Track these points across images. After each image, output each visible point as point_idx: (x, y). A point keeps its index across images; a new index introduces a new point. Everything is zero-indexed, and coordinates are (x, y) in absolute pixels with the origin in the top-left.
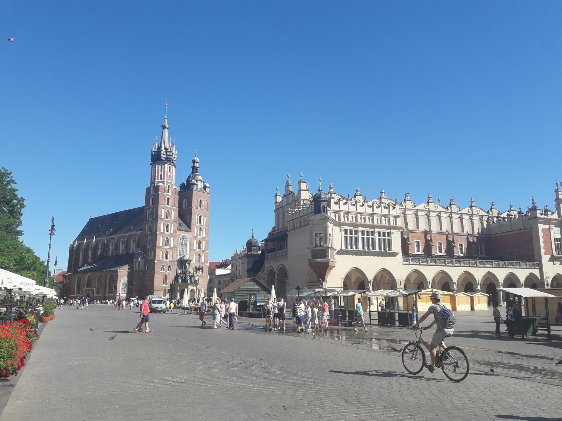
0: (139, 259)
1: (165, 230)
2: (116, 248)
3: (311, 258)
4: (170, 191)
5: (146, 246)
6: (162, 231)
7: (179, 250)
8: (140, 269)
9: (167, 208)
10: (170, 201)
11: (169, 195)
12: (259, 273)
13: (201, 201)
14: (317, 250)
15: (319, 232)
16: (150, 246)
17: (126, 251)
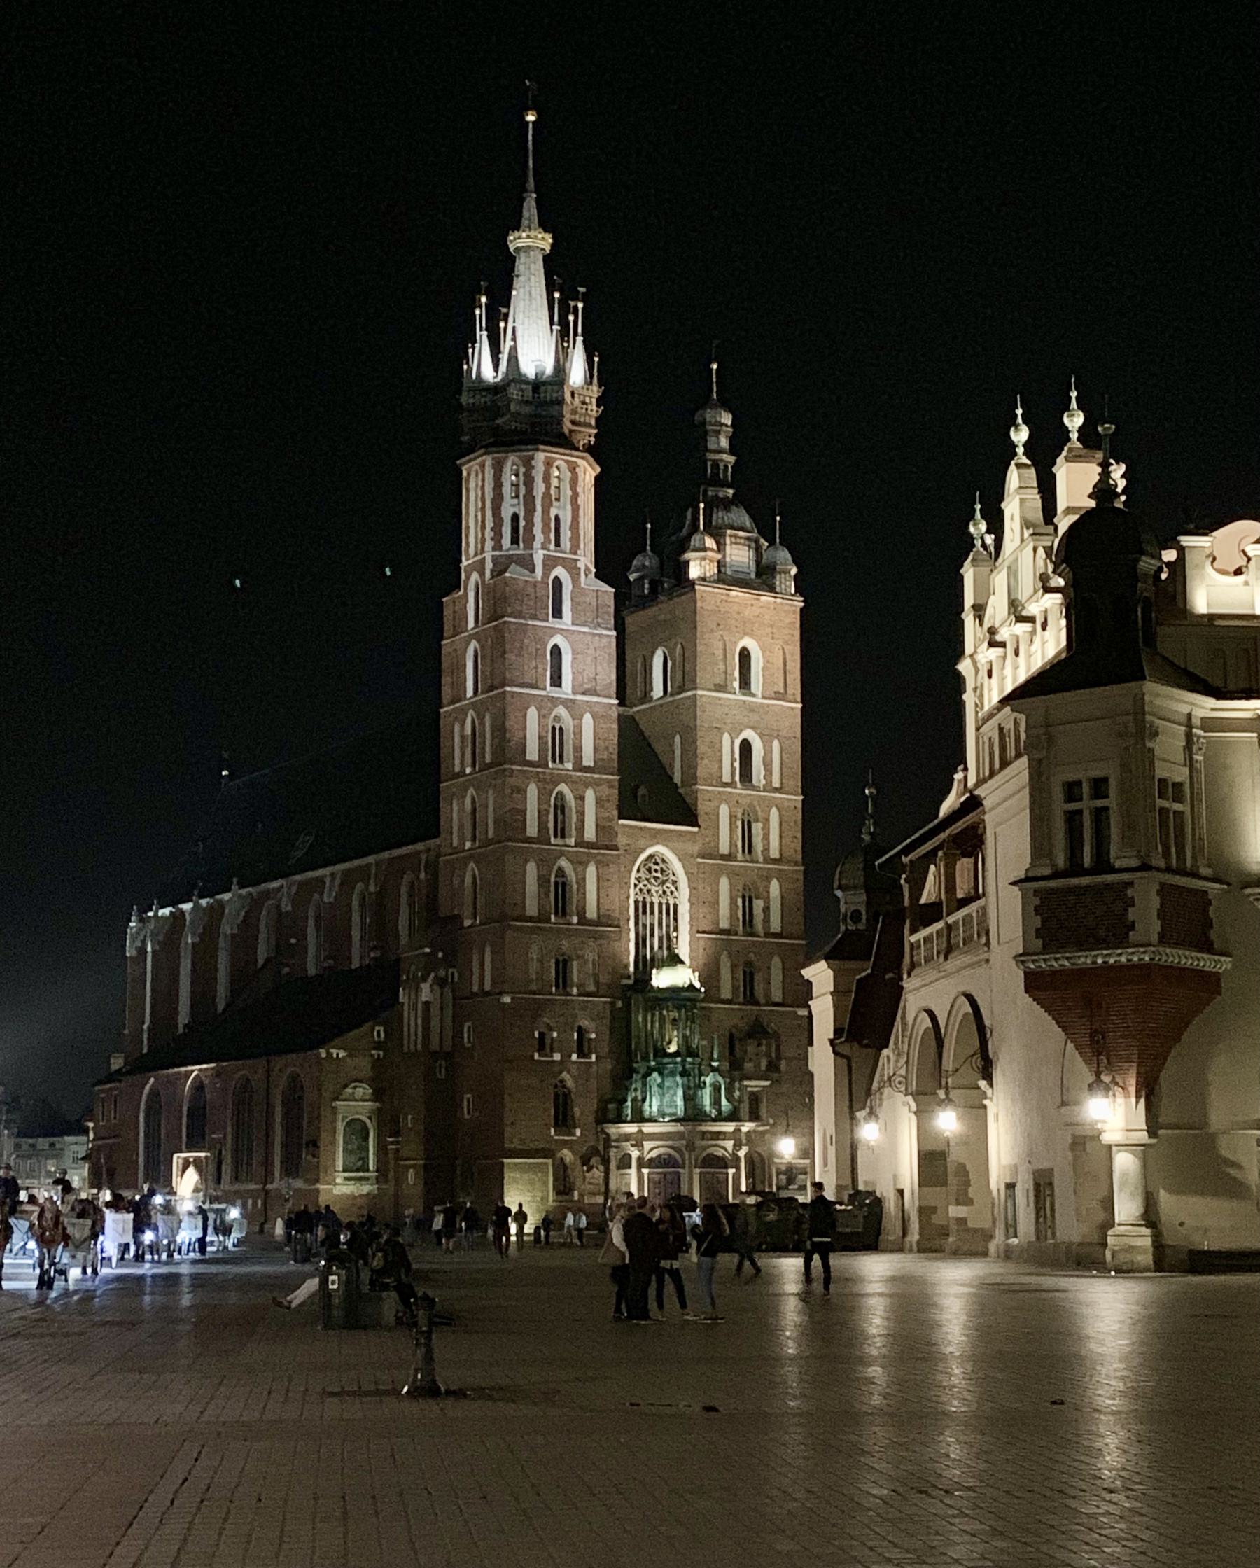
0: (426, 992)
1: (551, 825)
3: (1040, 942)
5: (458, 918)
8: (435, 1044)
9: (555, 702)
11: (560, 631)
12: (885, 1052)
13: (745, 656)
14: (1071, 890)
15: (1084, 774)
16: (475, 918)
17: (375, 948)
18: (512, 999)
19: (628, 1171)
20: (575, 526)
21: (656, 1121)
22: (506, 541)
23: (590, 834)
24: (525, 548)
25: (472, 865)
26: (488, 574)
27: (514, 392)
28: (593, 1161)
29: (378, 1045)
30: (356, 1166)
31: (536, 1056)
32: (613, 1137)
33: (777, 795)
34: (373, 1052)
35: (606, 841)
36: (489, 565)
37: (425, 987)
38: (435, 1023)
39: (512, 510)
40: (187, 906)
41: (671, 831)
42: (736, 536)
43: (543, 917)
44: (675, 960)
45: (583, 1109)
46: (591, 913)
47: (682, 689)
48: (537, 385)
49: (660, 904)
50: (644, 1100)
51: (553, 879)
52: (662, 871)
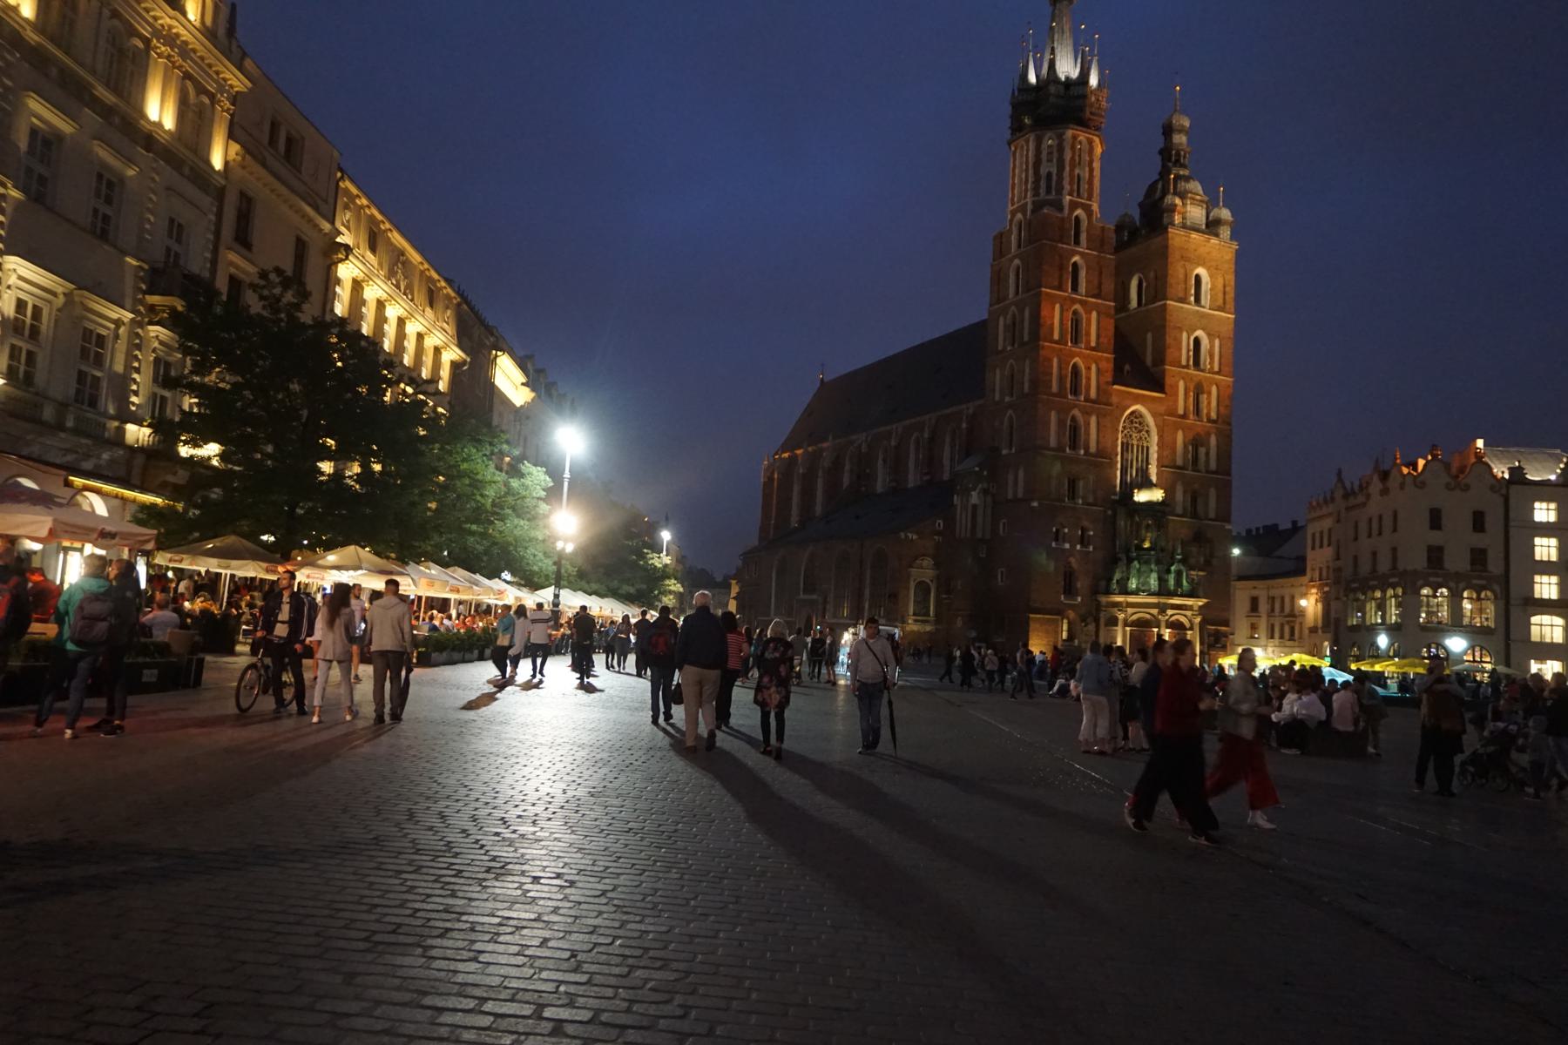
0: (975, 498)
1: (1068, 386)
4: (1083, 236)
6: (1055, 388)
7: (1119, 466)
8: (979, 535)
9: (1074, 301)
10: (1083, 274)
13: (1198, 278)
17: (926, 474)
20: (1091, 182)
21: (1137, 594)
22: (1042, 191)
23: (1093, 394)
26: (1029, 213)
27: (1052, 89)
28: (1089, 620)
29: (938, 533)
30: (921, 612)
31: (1054, 544)
33: (1217, 377)
34: (936, 537)
35: (1103, 399)
36: (1030, 207)
38: (980, 519)
40: (799, 452)
42: (1193, 199)
43: (1060, 448)
44: (1146, 484)
45: (1081, 584)
46: (1093, 449)
47: (1155, 299)
49: (1138, 446)
50: (1128, 579)
52: (1140, 424)
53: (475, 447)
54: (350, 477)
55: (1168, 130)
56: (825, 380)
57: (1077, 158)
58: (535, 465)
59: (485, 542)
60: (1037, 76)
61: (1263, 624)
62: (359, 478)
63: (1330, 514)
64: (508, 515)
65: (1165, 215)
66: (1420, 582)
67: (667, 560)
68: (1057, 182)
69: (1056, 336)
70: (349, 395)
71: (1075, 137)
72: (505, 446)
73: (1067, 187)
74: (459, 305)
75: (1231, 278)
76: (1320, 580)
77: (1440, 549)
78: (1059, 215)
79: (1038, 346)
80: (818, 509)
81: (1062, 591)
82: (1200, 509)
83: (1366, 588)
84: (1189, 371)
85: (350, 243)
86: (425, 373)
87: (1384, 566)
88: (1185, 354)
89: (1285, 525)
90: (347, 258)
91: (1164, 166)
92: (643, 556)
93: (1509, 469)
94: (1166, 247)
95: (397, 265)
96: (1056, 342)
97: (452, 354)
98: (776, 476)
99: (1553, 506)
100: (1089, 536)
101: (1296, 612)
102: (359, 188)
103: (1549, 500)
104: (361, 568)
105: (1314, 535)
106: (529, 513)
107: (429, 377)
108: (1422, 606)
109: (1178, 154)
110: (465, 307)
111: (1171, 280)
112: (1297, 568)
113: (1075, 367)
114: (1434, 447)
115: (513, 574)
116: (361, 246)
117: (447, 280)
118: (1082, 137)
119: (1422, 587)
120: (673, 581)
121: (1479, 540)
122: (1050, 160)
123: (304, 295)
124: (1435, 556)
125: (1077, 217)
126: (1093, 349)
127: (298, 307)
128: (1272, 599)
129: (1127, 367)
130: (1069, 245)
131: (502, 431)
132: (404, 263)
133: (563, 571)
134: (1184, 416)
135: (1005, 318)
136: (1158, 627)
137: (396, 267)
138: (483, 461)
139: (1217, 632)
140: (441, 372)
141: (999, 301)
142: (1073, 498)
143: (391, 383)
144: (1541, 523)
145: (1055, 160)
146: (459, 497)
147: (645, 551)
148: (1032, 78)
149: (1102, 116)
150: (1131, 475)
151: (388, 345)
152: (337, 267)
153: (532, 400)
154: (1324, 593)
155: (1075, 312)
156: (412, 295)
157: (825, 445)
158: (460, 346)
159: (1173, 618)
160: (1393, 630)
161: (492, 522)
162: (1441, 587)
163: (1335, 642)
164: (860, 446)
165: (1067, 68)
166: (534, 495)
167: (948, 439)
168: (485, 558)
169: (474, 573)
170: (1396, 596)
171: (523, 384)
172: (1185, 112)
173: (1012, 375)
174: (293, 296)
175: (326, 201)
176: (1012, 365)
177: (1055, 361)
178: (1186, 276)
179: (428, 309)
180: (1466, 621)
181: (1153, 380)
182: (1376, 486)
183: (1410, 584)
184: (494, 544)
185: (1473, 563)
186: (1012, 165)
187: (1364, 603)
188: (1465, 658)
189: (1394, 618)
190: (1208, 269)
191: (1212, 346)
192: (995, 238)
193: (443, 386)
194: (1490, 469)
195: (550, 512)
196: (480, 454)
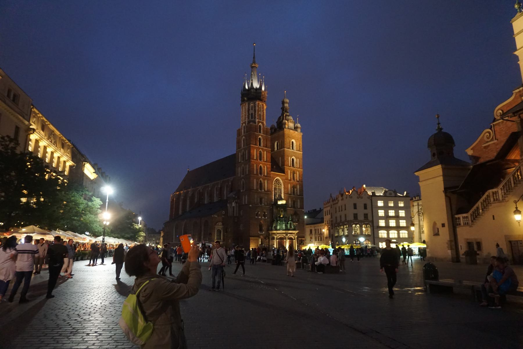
0: (234, 204)
1: (259, 172)
2: (211, 196)
5: (239, 190)
6: (255, 173)
7: (273, 194)
8: (235, 215)
9: (260, 148)
10: (262, 141)
11: (260, 135)
13: (293, 142)
16: (243, 190)
17: (220, 198)
18: (252, 206)
19: (274, 240)
22: (250, 118)
23: (266, 174)
24: (254, 119)
25: (243, 179)
26: (247, 124)
27: (252, 90)
28: (267, 238)
29: (224, 215)
31: (256, 217)
32: (271, 233)
34: (223, 216)
36: (247, 122)
37: (233, 203)
38: (235, 210)
39: (251, 112)
40: (182, 192)
41: (280, 175)
43: (257, 190)
44: (281, 199)
45: (264, 228)
46: (266, 189)
48: (256, 89)
49: (278, 189)
51: (259, 183)
52: (279, 182)
53: (76, 192)
54: (32, 203)
55: (283, 103)
56: (189, 171)
57: (259, 109)
58: (97, 198)
59: (79, 222)
60: (248, 87)
61: (313, 237)
62: (35, 203)
63: (329, 206)
64: (87, 214)
65: (283, 125)
66: (352, 223)
67: (140, 226)
68: (254, 115)
69: (255, 158)
70: (32, 177)
71: (259, 104)
72: (87, 193)
73: (256, 116)
74: (72, 148)
75: (301, 142)
76: (328, 224)
77: (356, 214)
78: (255, 125)
79: (250, 161)
80: (188, 209)
81: (259, 230)
82: (296, 205)
83: (339, 226)
84: (291, 168)
85: (35, 128)
86: (60, 169)
87: (343, 219)
88: (290, 163)
89: (318, 209)
90: (33, 133)
91: (282, 112)
92: (132, 225)
93: (372, 192)
94: (284, 134)
95: (51, 135)
96: (255, 160)
97: (70, 163)
98: (175, 199)
99: (382, 202)
100: (266, 214)
101: (322, 233)
102: (38, 111)
103: (381, 200)
104: (34, 233)
105: (325, 212)
106: (94, 213)
107: (62, 170)
108: (353, 230)
109: (286, 109)
110: (74, 148)
111: (285, 143)
112: (322, 222)
113: (260, 167)
114: (354, 187)
115: (89, 233)
116: (39, 129)
117: (68, 140)
118: (261, 104)
119: (353, 225)
120: (142, 233)
121: (366, 211)
122: (252, 110)
123: (17, 144)
124: (356, 216)
125: (260, 126)
126: (265, 162)
127: (15, 148)
128: (315, 230)
129: (275, 167)
130: (258, 133)
131: (86, 187)
132: (54, 135)
133: (106, 231)
134: (290, 180)
135: (241, 153)
136: (286, 239)
137: (51, 136)
138: (79, 197)
139: (301, 240)
140: (66, 169)
141: (239, 148)
142: (261, 204)
143: (48, 172)
144: (380, 206)
145: (253, 109)
146: (71, 208)
147: (133, 223)
148: (247, 87)
149: (265, 98)
150: (277, 197)
151: (47, 160)
152: (30, 136)
153: (97, 177)
154: (329, 227)
155: (260, 152)
156: (56, 144)
157: (189, 190)
158: (73, 160)
159: (290, 237)
160: (346, 236)
161: (82, 216)
162: (357, 224)
163: (332, 241)
164: (200, 190)
165: (256, 85)
166: (96, 207)
167: (225, 188)
168: (79, 228)
169: (75, 233)
170: (346, 227)
171: (94, 172)
172: (288, 98)
173: (243, 169)
174: (13, 144)
175: (27, 115)
176: (243, 166)
177: (255, 165)
178: (289, 142)
179: (62, 149)
180: (364, 233)
181: (283, 171)
182: (340, 198)
183: (350, 224)
184: (83, 223)
185: (365, 217)
186: (242, 111)
187: (339, 230)
188: (364, 243)
189: (346, 233)
190: (295, 140)
191: (297, 161)
192: (237, 131)
193: (66, 173)
194: (367, 192)
195: (102, 213)
196: (78, 194)
